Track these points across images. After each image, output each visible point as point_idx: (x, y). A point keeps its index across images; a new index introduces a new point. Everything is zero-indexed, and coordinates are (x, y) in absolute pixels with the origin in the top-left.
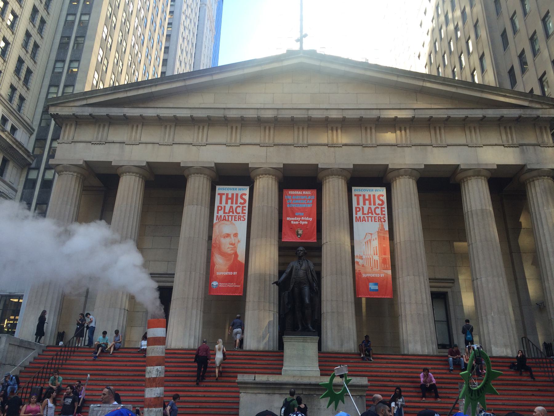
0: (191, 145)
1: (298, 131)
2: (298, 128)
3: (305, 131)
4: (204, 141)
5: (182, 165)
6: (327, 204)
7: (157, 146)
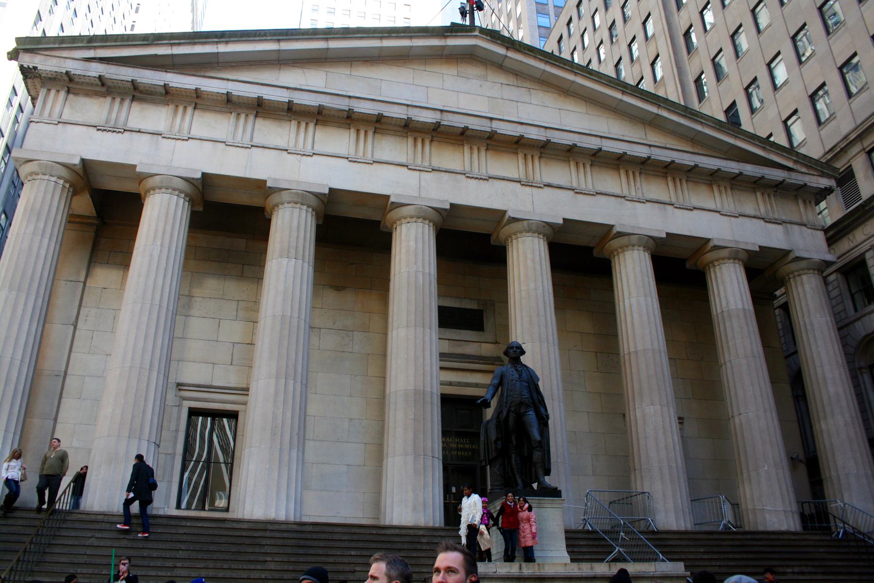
3: (483, 153)
4: (309, 147)
5: (269, 184)
6: (522, 279)
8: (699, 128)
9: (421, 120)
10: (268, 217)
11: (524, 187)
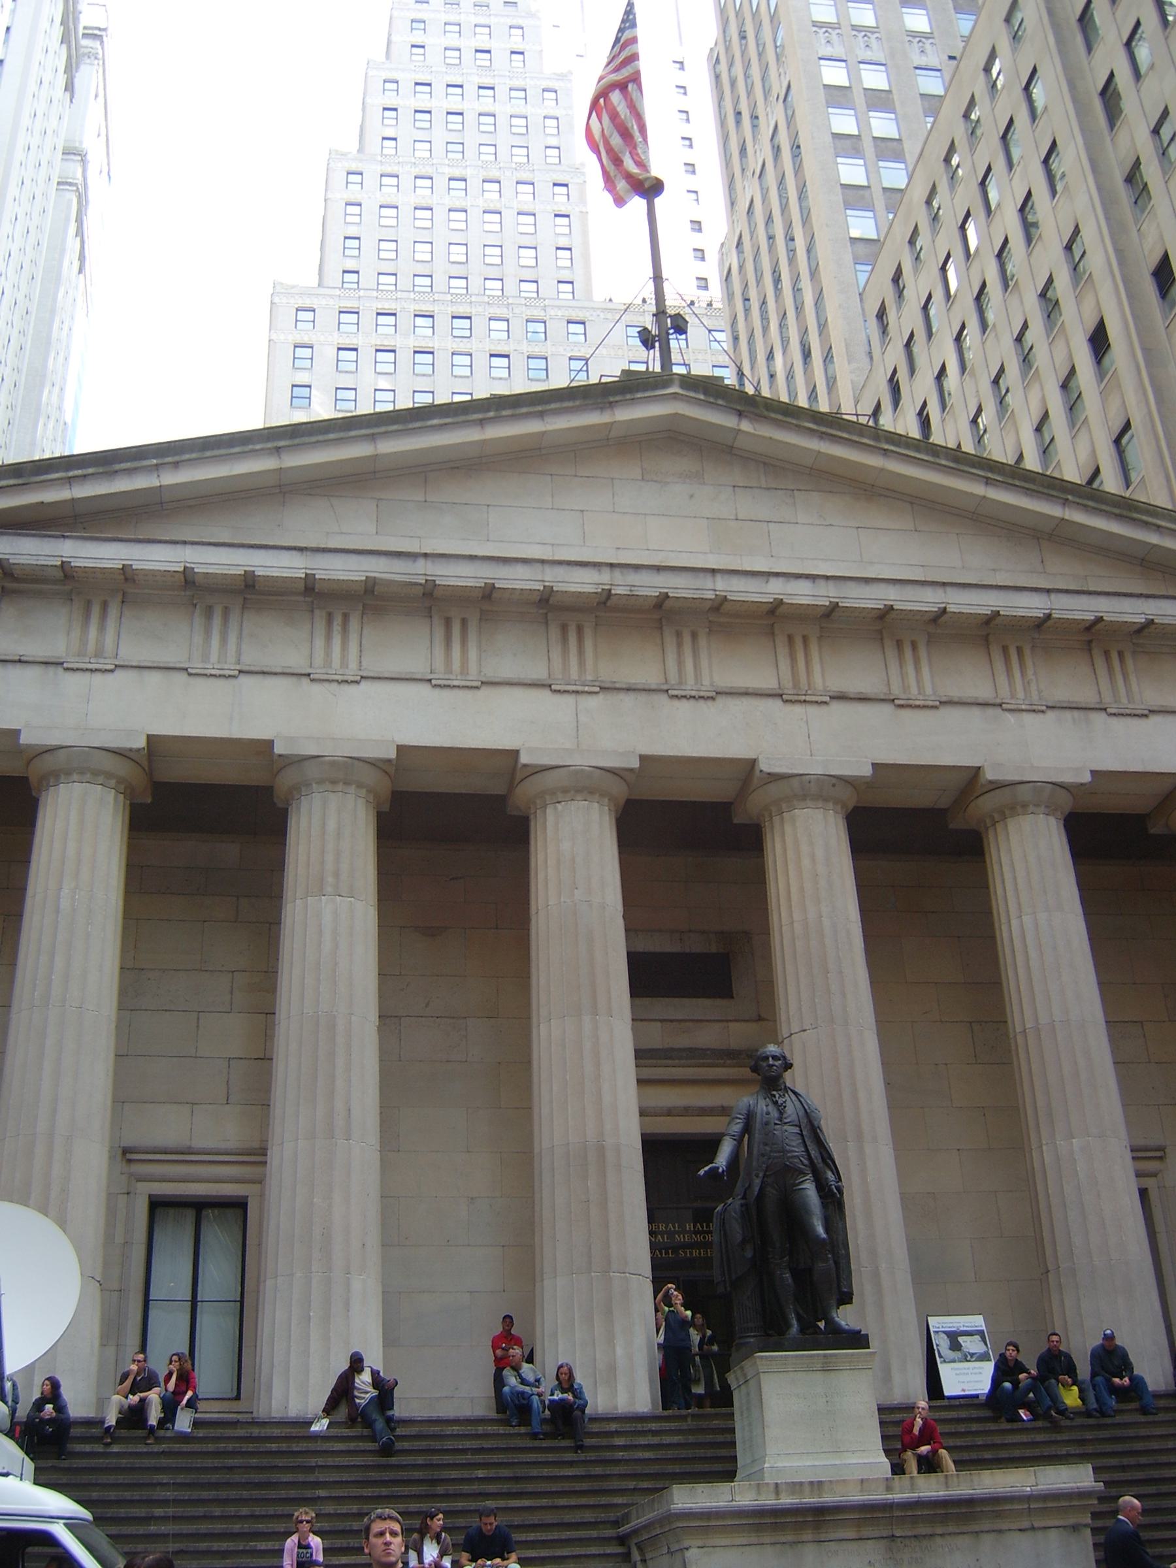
0: (305, 681)
1: (680, 645)
2: (679, 635)
4: (353, 665)
6: (795, 897)
7: (183, 676)
8: (1153, 539)
9: (573, 588)
10: (280, 805)
11: (790, 708)
